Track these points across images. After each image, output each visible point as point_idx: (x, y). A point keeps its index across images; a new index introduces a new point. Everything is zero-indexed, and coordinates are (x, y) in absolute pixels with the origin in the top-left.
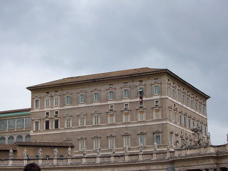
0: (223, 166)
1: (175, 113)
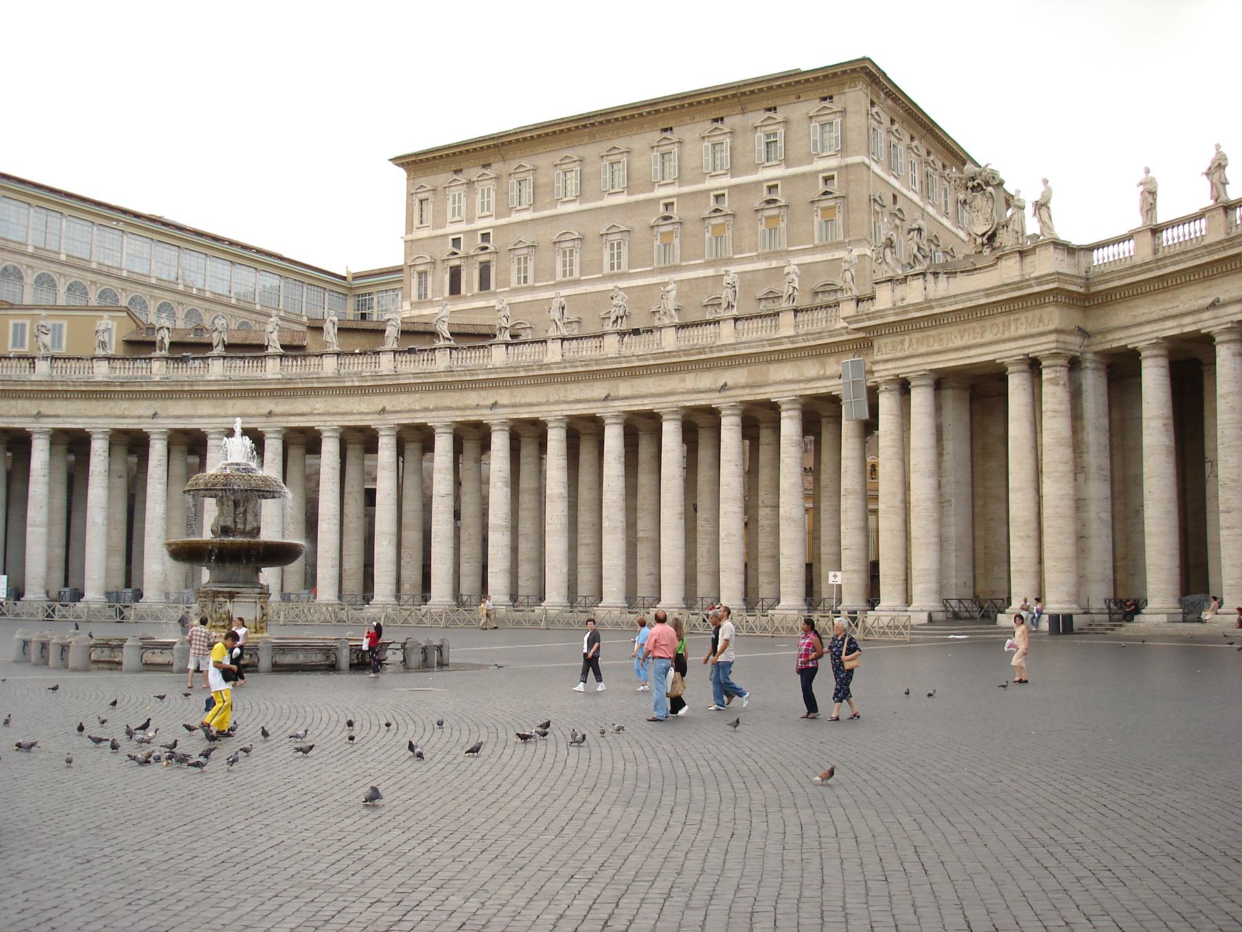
0: (1114, 340)
1: (897, 227)
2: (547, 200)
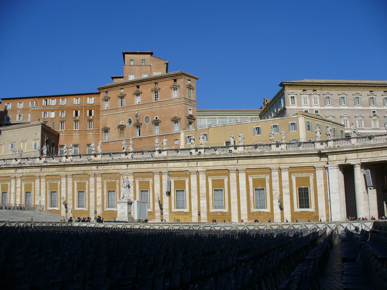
2: (337, 104)
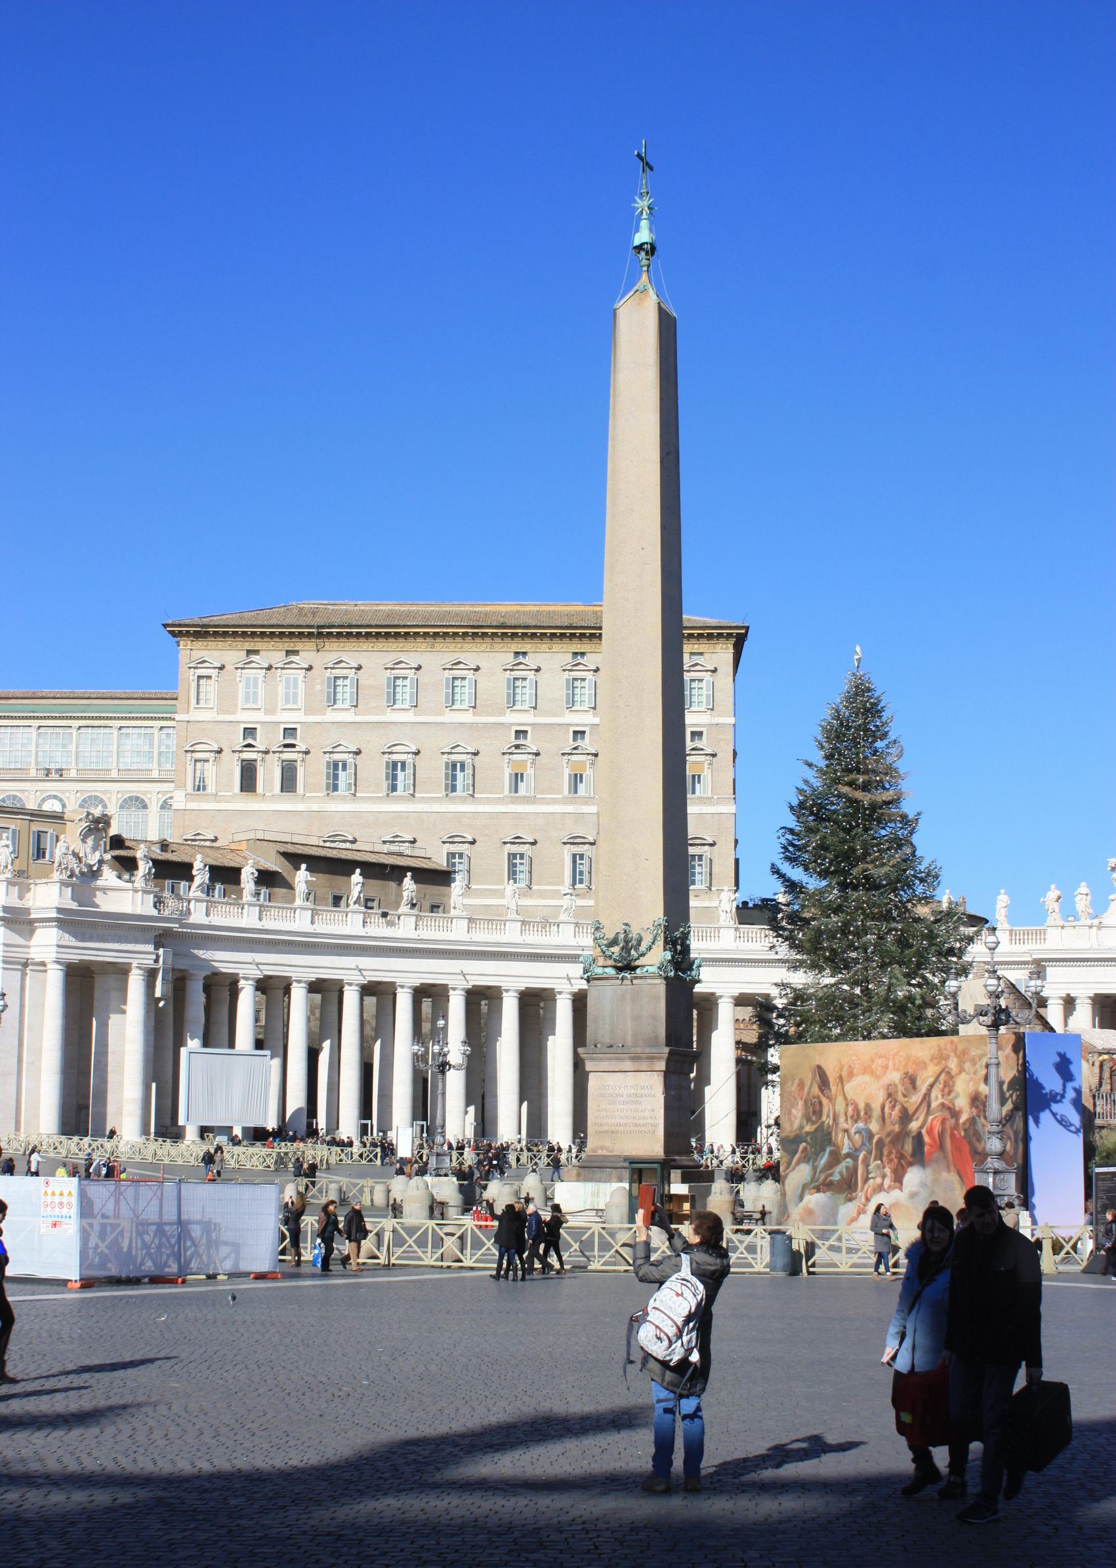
2: (374, 704)
